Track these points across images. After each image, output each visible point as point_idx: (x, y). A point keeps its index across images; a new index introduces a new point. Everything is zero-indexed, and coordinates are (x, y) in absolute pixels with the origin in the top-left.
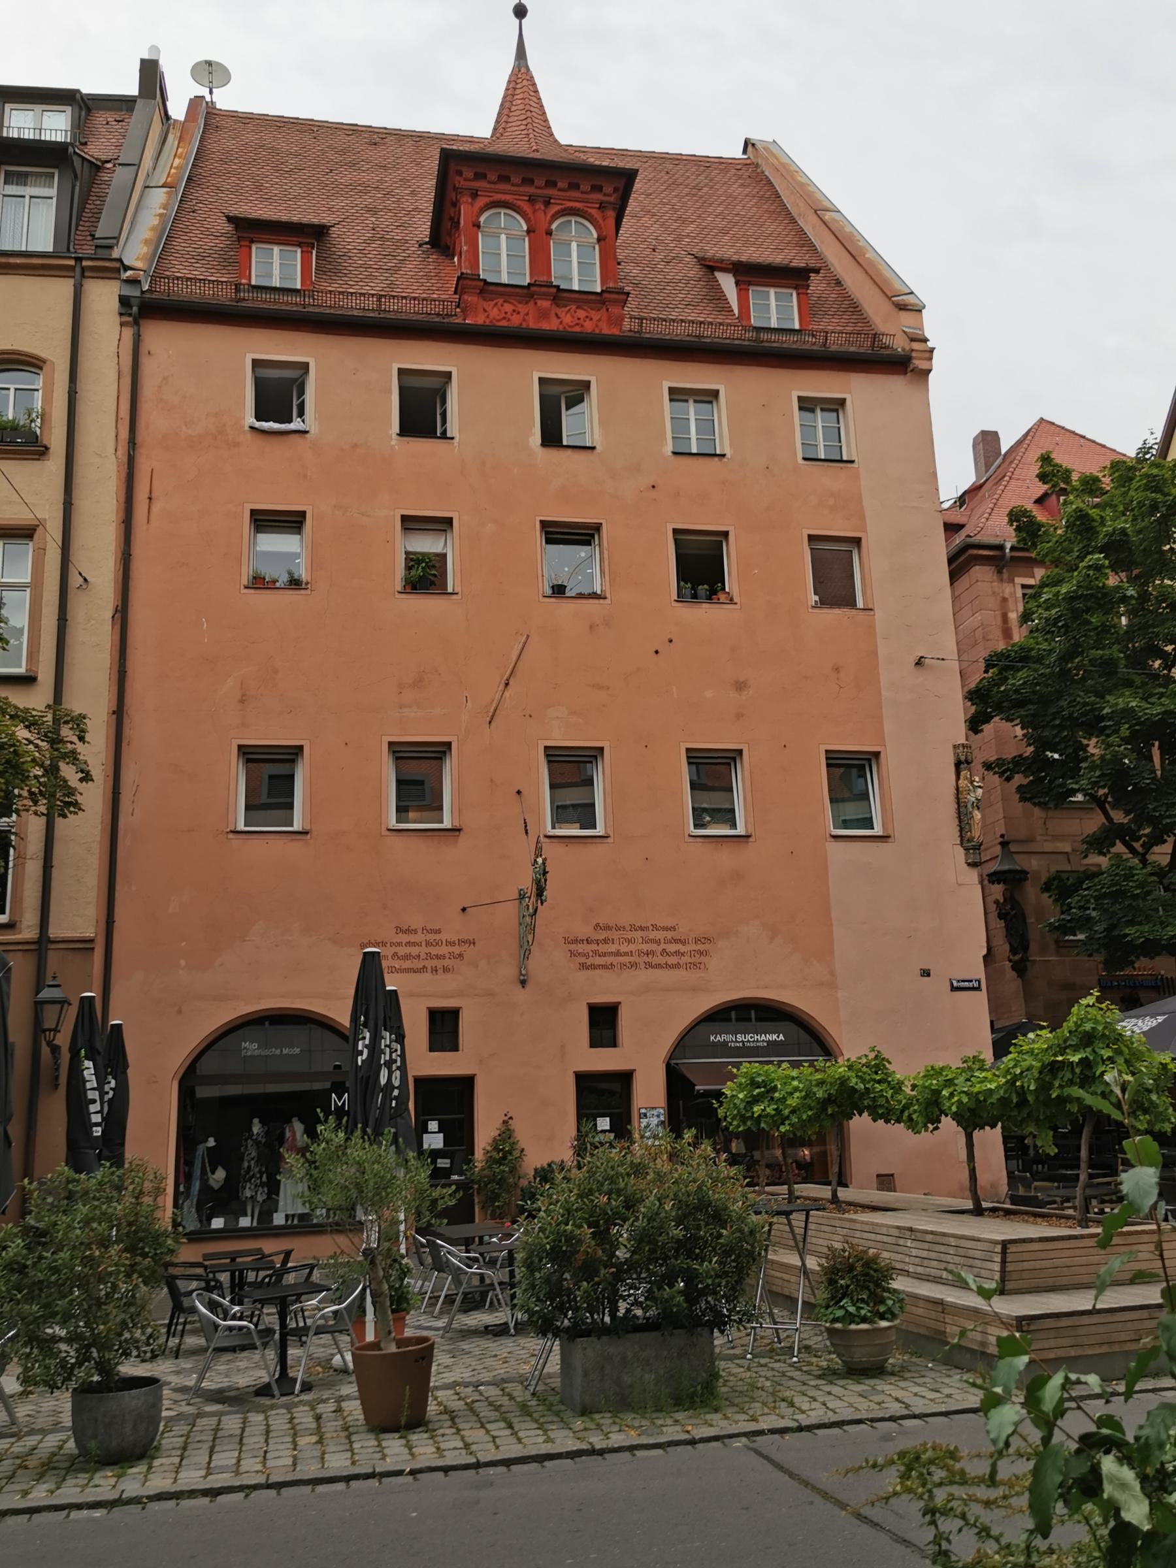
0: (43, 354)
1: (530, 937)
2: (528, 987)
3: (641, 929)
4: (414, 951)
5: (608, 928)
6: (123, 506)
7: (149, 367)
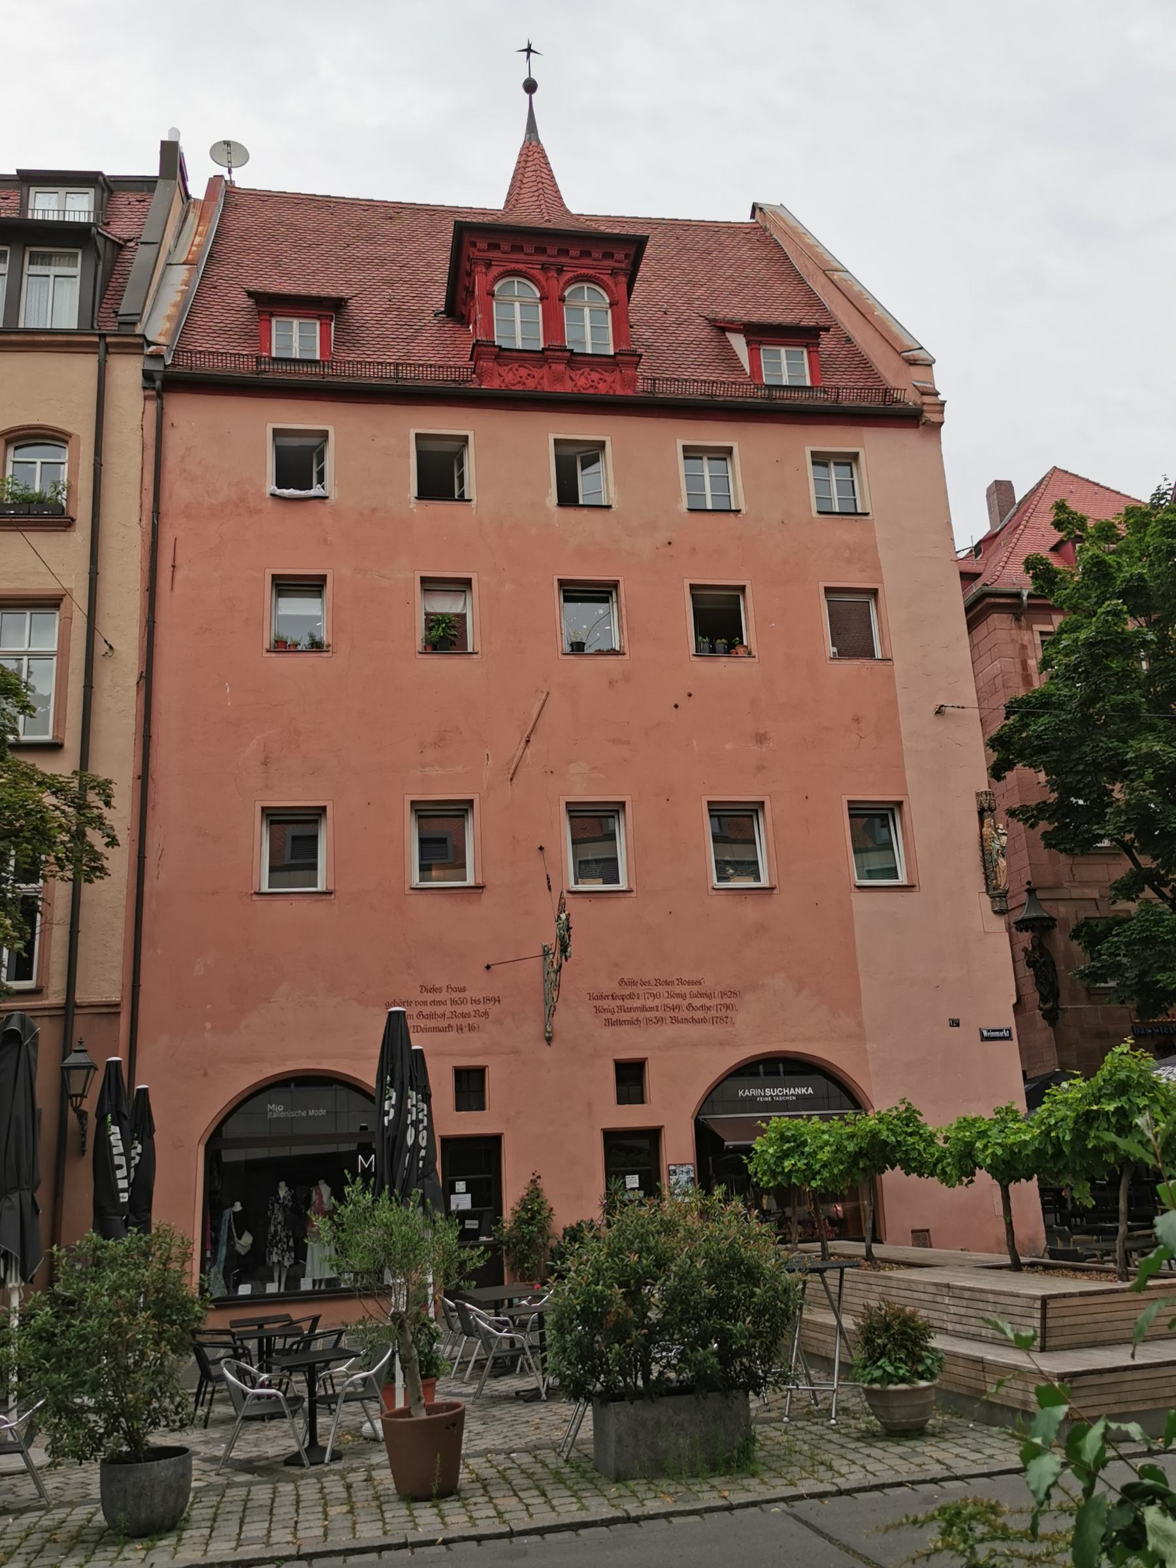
0: (69, 429)
1: (555, 994)
2: (553, 1044)
3: (667, 983)
4: (439, 1010)
5: (633, 983)
6: (147, 574)
7: (173, 440)
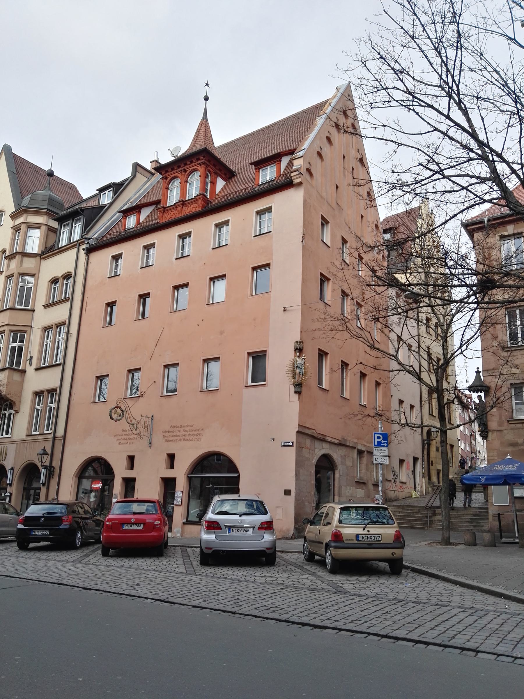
2: (151, 448)
3: (184, 427)
4: (125, 437)
5: (174, 427)
